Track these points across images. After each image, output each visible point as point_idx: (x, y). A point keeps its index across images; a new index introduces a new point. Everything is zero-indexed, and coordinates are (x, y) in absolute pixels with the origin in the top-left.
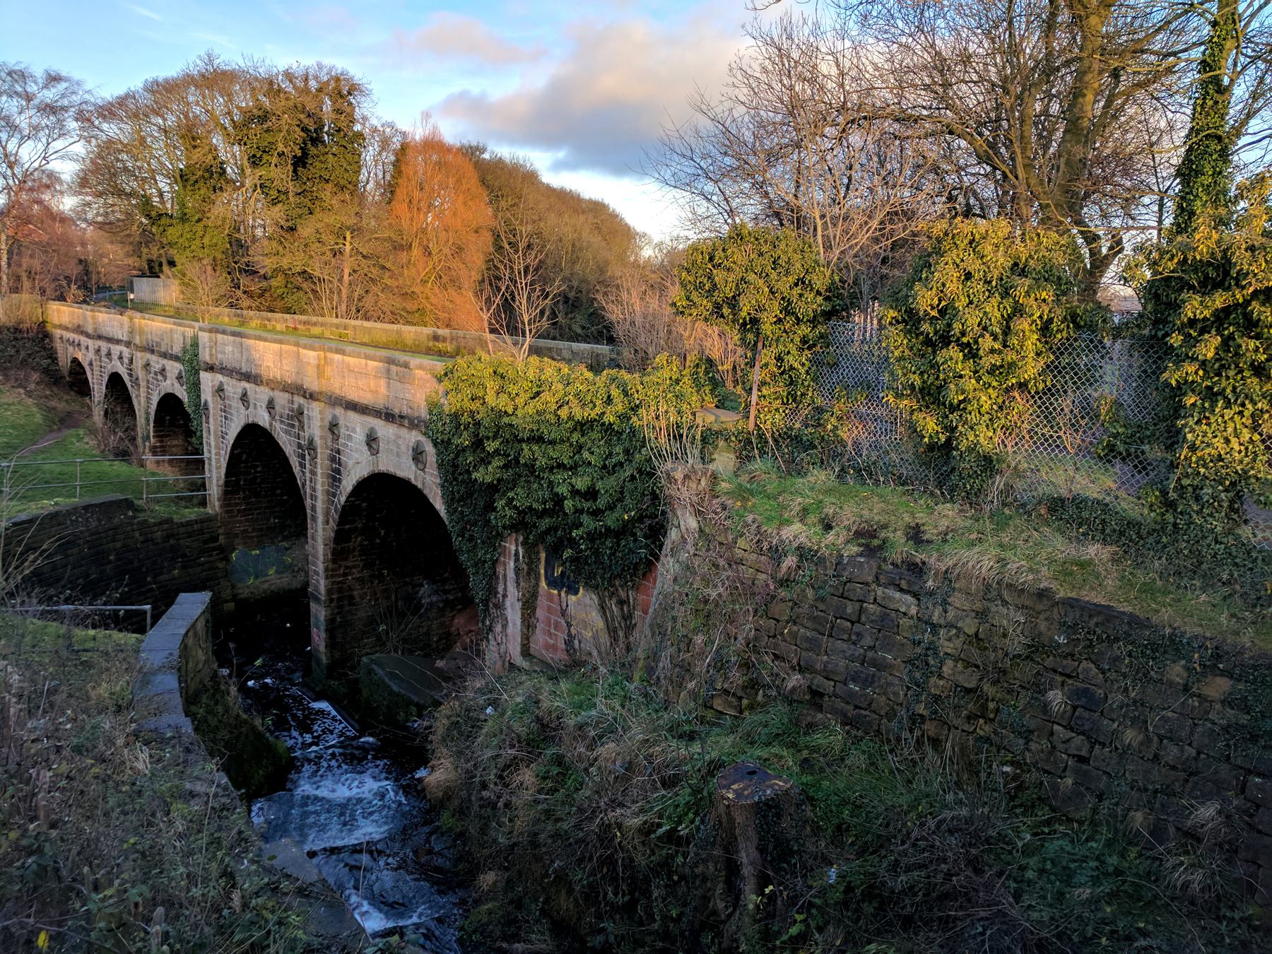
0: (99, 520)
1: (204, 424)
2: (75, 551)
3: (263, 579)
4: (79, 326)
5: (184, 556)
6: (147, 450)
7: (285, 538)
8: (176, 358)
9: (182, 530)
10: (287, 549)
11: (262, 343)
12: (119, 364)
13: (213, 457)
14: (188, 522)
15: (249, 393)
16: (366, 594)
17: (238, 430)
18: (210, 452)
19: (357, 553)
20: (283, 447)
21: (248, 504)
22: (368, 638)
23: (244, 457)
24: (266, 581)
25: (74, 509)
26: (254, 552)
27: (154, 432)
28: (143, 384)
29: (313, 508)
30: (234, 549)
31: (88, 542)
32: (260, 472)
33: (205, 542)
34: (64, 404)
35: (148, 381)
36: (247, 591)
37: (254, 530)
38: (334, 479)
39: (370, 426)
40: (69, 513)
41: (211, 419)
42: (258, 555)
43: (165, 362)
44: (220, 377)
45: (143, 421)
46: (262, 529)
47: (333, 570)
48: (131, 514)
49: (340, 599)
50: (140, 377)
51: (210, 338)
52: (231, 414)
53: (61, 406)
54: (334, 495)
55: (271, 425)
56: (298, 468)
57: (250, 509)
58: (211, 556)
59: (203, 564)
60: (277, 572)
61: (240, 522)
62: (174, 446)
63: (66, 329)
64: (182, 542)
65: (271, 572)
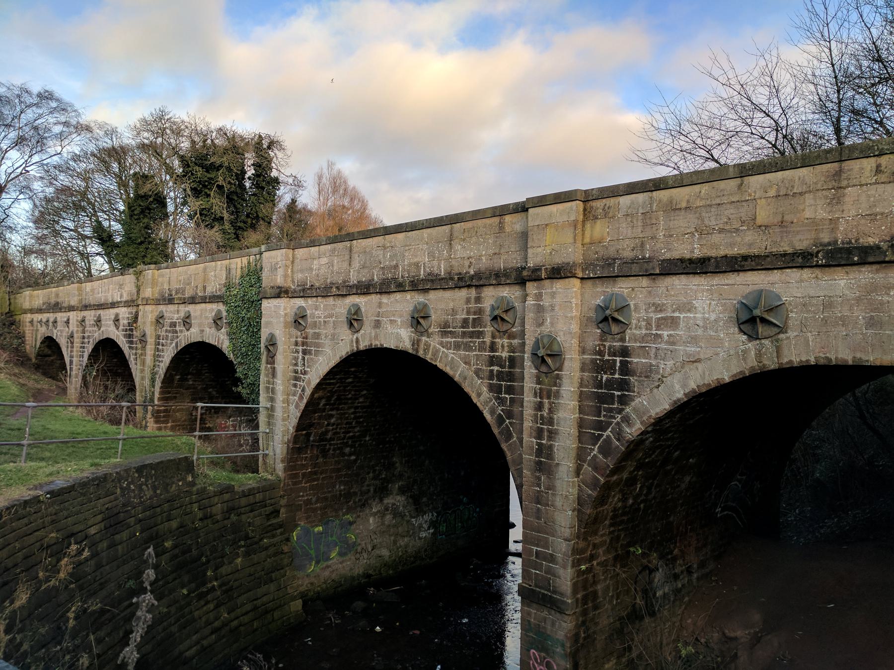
0: (155, 488)
1: (263, 366)
2: (125, 535)
3: (325, 564)
4: (57, 304)
5: (247, 538)
6: (149, 415)
7: (349, 510)
8: (214, 299)
9: (244, 501)
10: (351, 523)
11: (401, 236)
12: (112, 328)
13: (279, 405)
14: (250, 490)
15: (363, 310)
16: (608, 587)
17: (332, 363)
18: (272, 400)
19: (607, 522)
20: (448, 370)
21: (315, 465)
22: (609, 660)
23: (323, 402)
24: (328, 567)
25: (126, 471)
26: (316, 529)
27: (161, 393)
28: (151, 340)
29: (544, 452)
30: (296, 526)
31: (140, 521)
32: (333, 424)
33: (268, 517)
34: (32, 382)
35: (158, 337)
36: (307, 581)
37: (316, 502)
38: (603, 399)
39: (751, 288)
40: (119, 478)
41: (279, 358)
42: (320, 533)
43: (191, 308)
44: (300, 302)
45: (147, 382)
46: (326, 499)
47: (582, 551)
48: (190, 479)
49: (585, 599)
50: (148, 333)
51: (287, 255)
52: (317, 345)
53: (31, 384)
54: (601, 426)
55: (416, 343)
56: (486, 394)
57: (315, 473)
58: (274, 536)
59: (266, 549)
60: (340, 554)
61: (304, 489)
62: (178, 411)
63: (40, 311)
64: (244, 517)
65: (333, 555)
